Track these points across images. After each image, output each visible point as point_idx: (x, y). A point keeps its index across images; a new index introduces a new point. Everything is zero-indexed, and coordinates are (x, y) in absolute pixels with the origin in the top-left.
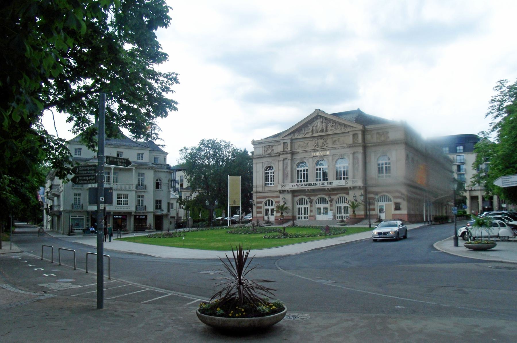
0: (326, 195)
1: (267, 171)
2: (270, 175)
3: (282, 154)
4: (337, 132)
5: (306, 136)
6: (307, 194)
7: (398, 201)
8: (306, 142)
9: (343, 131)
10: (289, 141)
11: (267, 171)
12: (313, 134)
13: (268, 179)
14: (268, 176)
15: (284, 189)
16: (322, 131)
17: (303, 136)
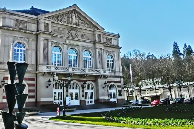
0: (79, 81)
1: (16, 48)
2: (19, 53)
3: (44, 33)
4: (85, 28)
5: (63, 23)
6: (63, 78)
7: (120, 89)
8: (61, 29)
9: (90, 29)
10: (50, 23)
11: (16, 48)
12: (68, 24)
13: (18, 57)
14: (18, 54)
15: (49, 70)
16: (76, 25)
17: (61, 23)
